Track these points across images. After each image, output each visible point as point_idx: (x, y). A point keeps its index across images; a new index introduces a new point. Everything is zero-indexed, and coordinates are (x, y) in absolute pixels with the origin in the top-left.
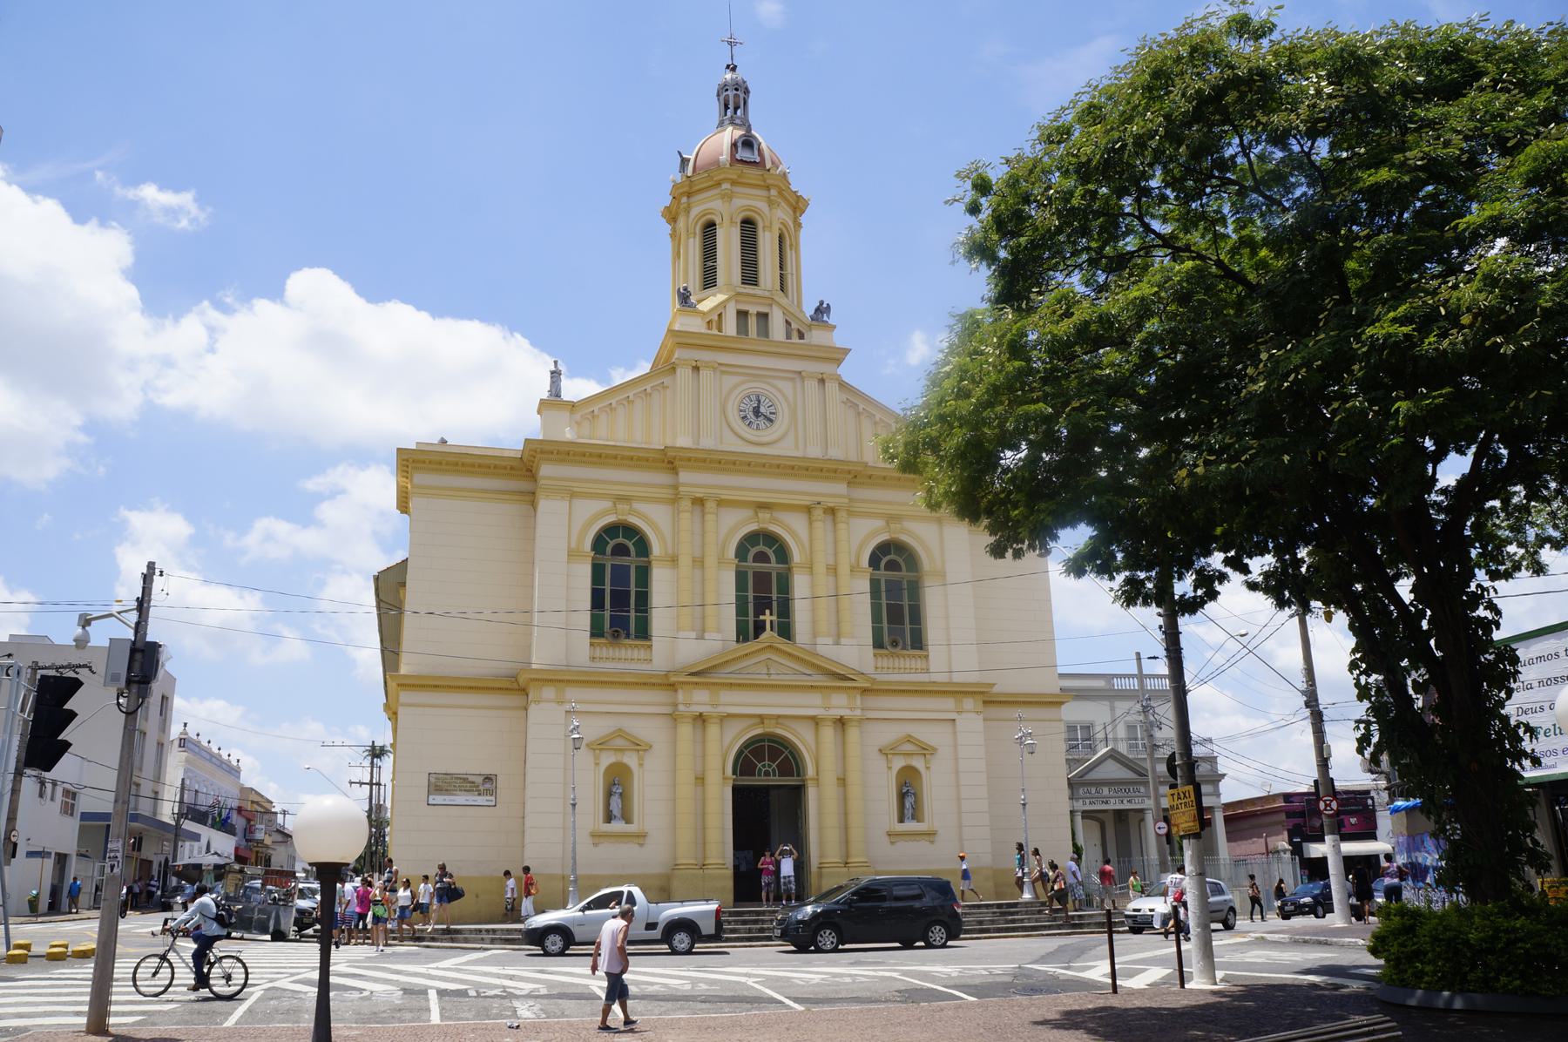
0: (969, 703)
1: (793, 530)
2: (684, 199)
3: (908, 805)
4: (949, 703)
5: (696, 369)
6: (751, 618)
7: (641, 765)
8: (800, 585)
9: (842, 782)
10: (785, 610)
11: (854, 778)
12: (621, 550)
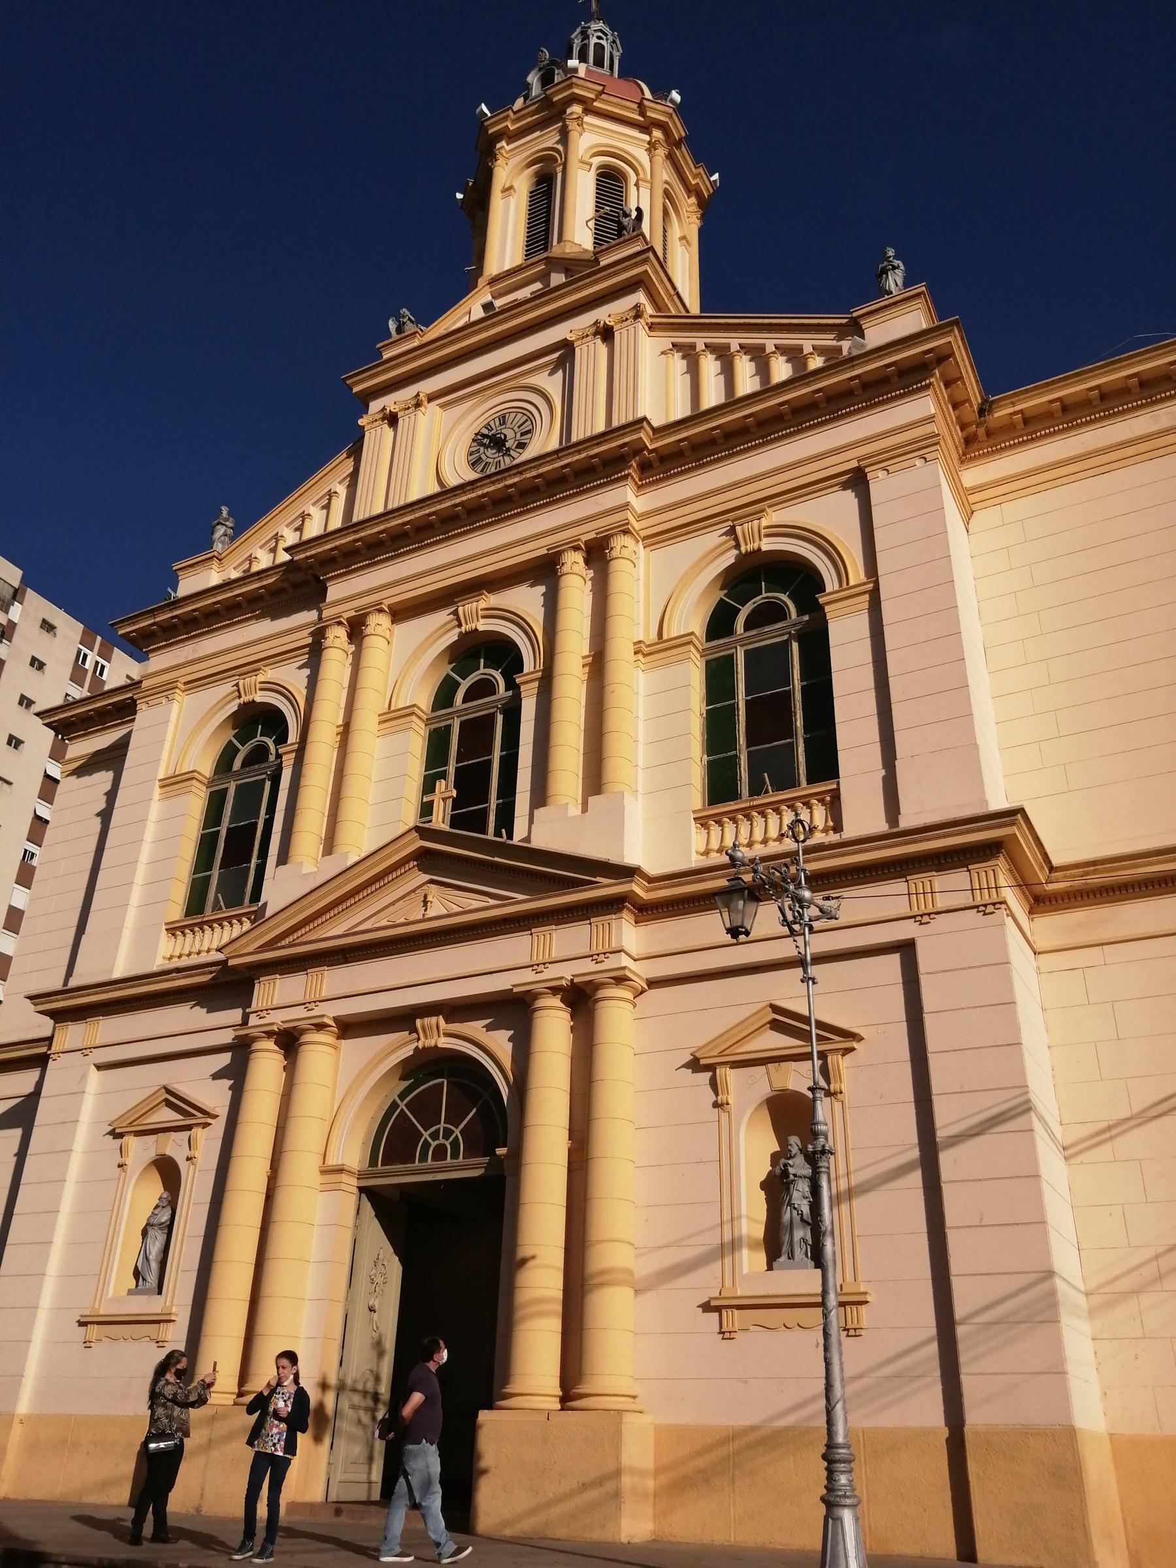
0: (951, 886)
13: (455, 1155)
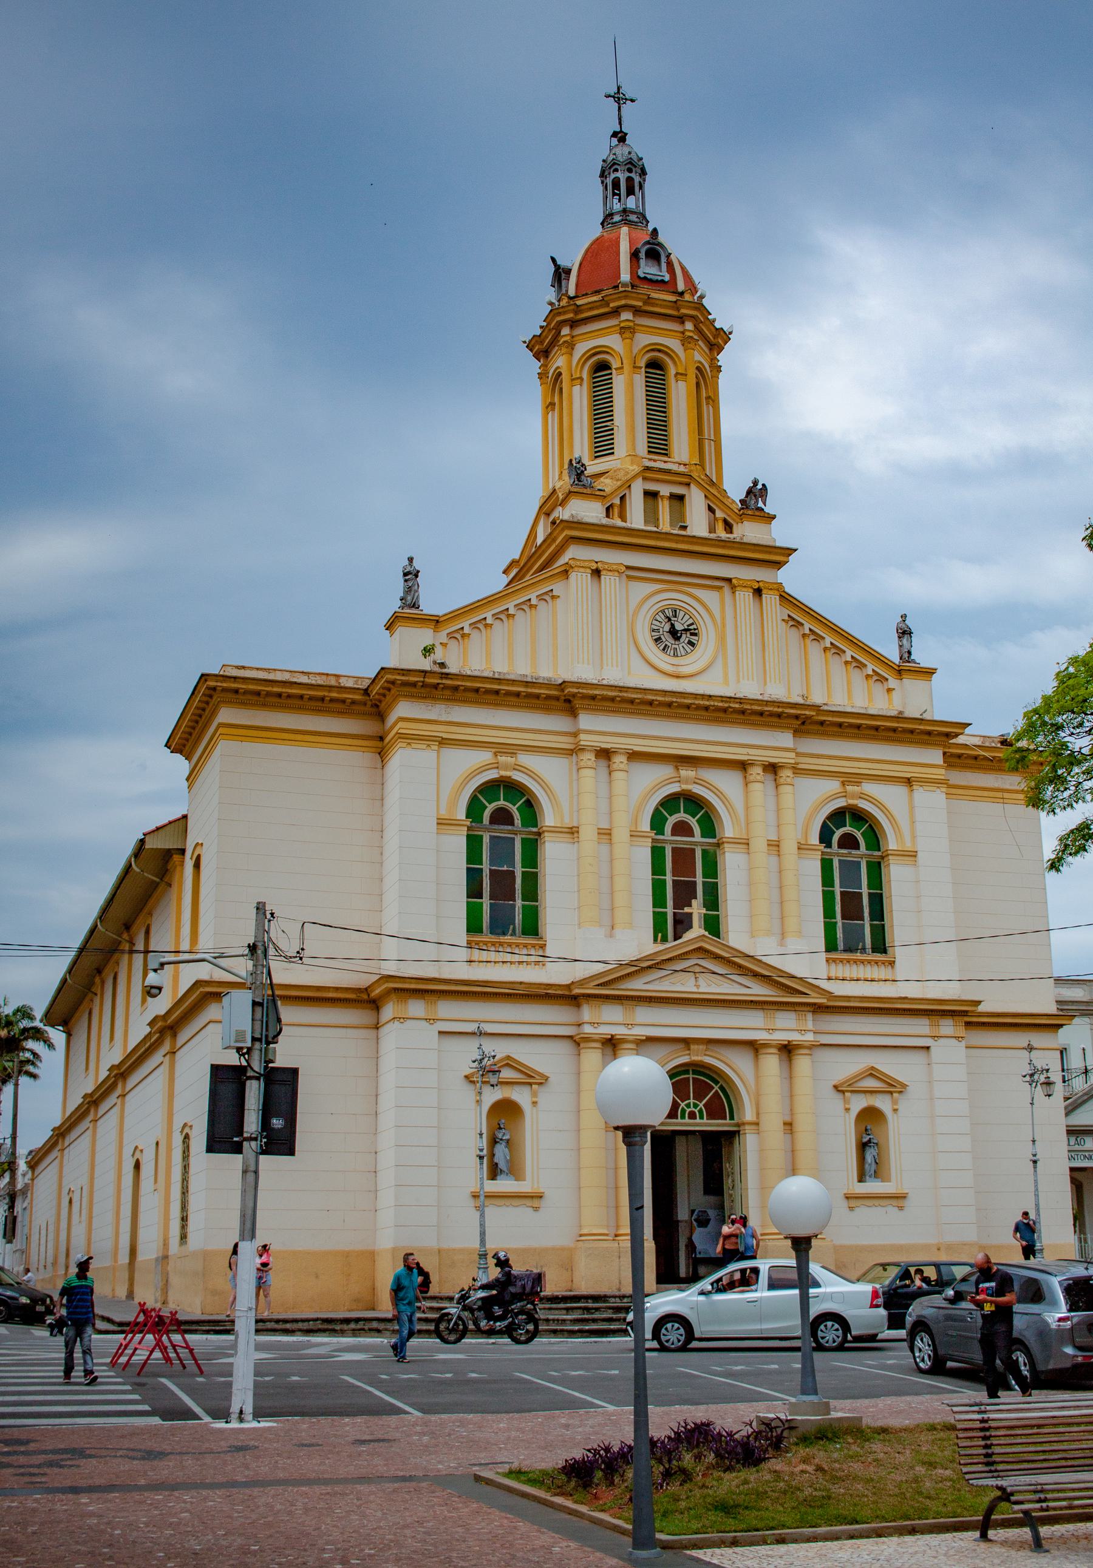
0: (947, 1027)
1: (723, 790)
2: (566, 331)
3: (869, 1158)
4: (921, 1026)
5: (597, 573)
6: (670, 910)
7: (535, 1103)
8: (733, 866)
9: (789, 1126)
10: (713, 900)
11: (803, 1123)
12: (502, 817)
13: (701, 1118)
